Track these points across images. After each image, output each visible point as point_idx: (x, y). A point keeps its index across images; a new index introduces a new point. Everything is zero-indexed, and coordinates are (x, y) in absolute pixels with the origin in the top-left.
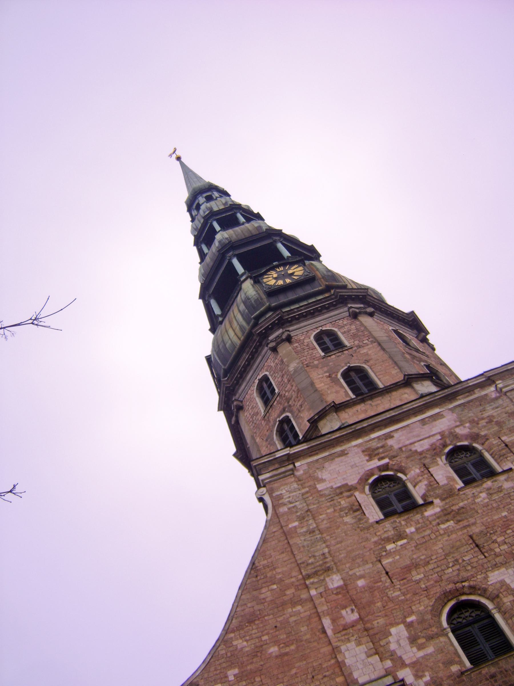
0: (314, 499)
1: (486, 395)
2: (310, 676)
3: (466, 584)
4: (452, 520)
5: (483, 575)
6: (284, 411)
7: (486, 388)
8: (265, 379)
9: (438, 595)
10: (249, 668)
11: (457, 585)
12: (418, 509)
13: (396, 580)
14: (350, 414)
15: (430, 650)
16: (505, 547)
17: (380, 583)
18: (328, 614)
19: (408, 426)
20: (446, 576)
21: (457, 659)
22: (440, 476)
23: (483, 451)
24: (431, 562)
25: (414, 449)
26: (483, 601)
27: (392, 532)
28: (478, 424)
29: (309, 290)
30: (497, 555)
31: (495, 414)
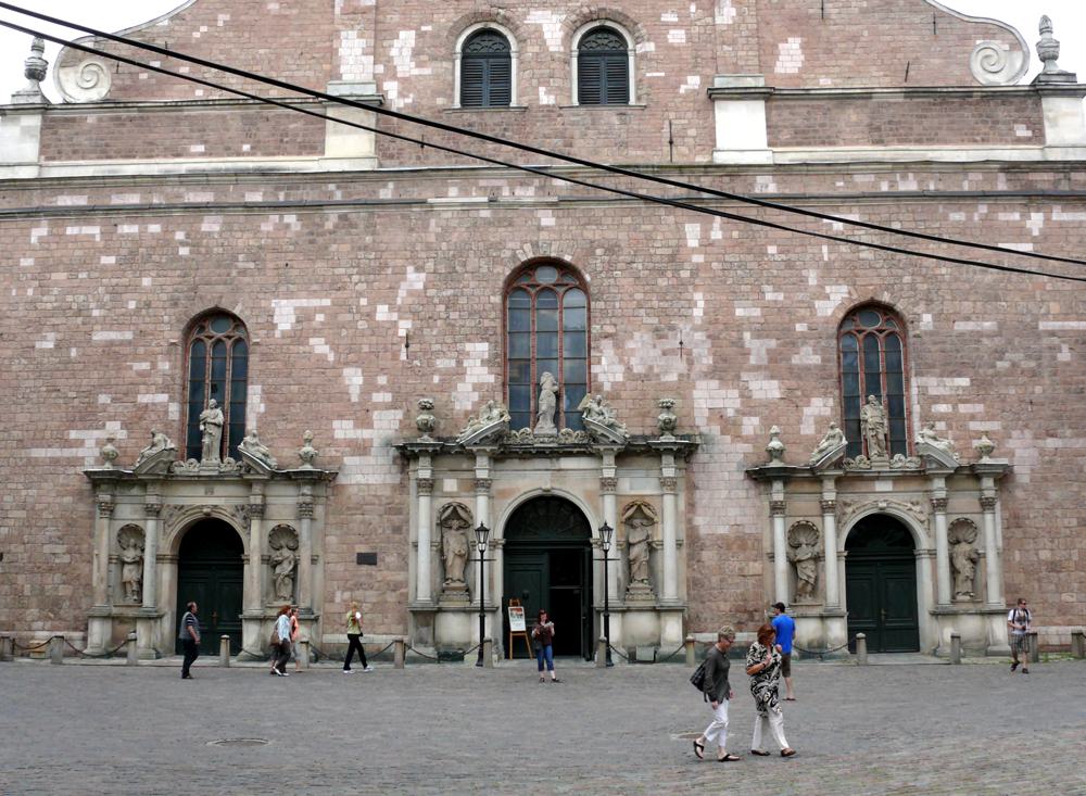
2: (299, 52)
5: (524, 10)
9: (467, 12)
15: (427, 71)
21: (449, 92)
26: (510, 38)
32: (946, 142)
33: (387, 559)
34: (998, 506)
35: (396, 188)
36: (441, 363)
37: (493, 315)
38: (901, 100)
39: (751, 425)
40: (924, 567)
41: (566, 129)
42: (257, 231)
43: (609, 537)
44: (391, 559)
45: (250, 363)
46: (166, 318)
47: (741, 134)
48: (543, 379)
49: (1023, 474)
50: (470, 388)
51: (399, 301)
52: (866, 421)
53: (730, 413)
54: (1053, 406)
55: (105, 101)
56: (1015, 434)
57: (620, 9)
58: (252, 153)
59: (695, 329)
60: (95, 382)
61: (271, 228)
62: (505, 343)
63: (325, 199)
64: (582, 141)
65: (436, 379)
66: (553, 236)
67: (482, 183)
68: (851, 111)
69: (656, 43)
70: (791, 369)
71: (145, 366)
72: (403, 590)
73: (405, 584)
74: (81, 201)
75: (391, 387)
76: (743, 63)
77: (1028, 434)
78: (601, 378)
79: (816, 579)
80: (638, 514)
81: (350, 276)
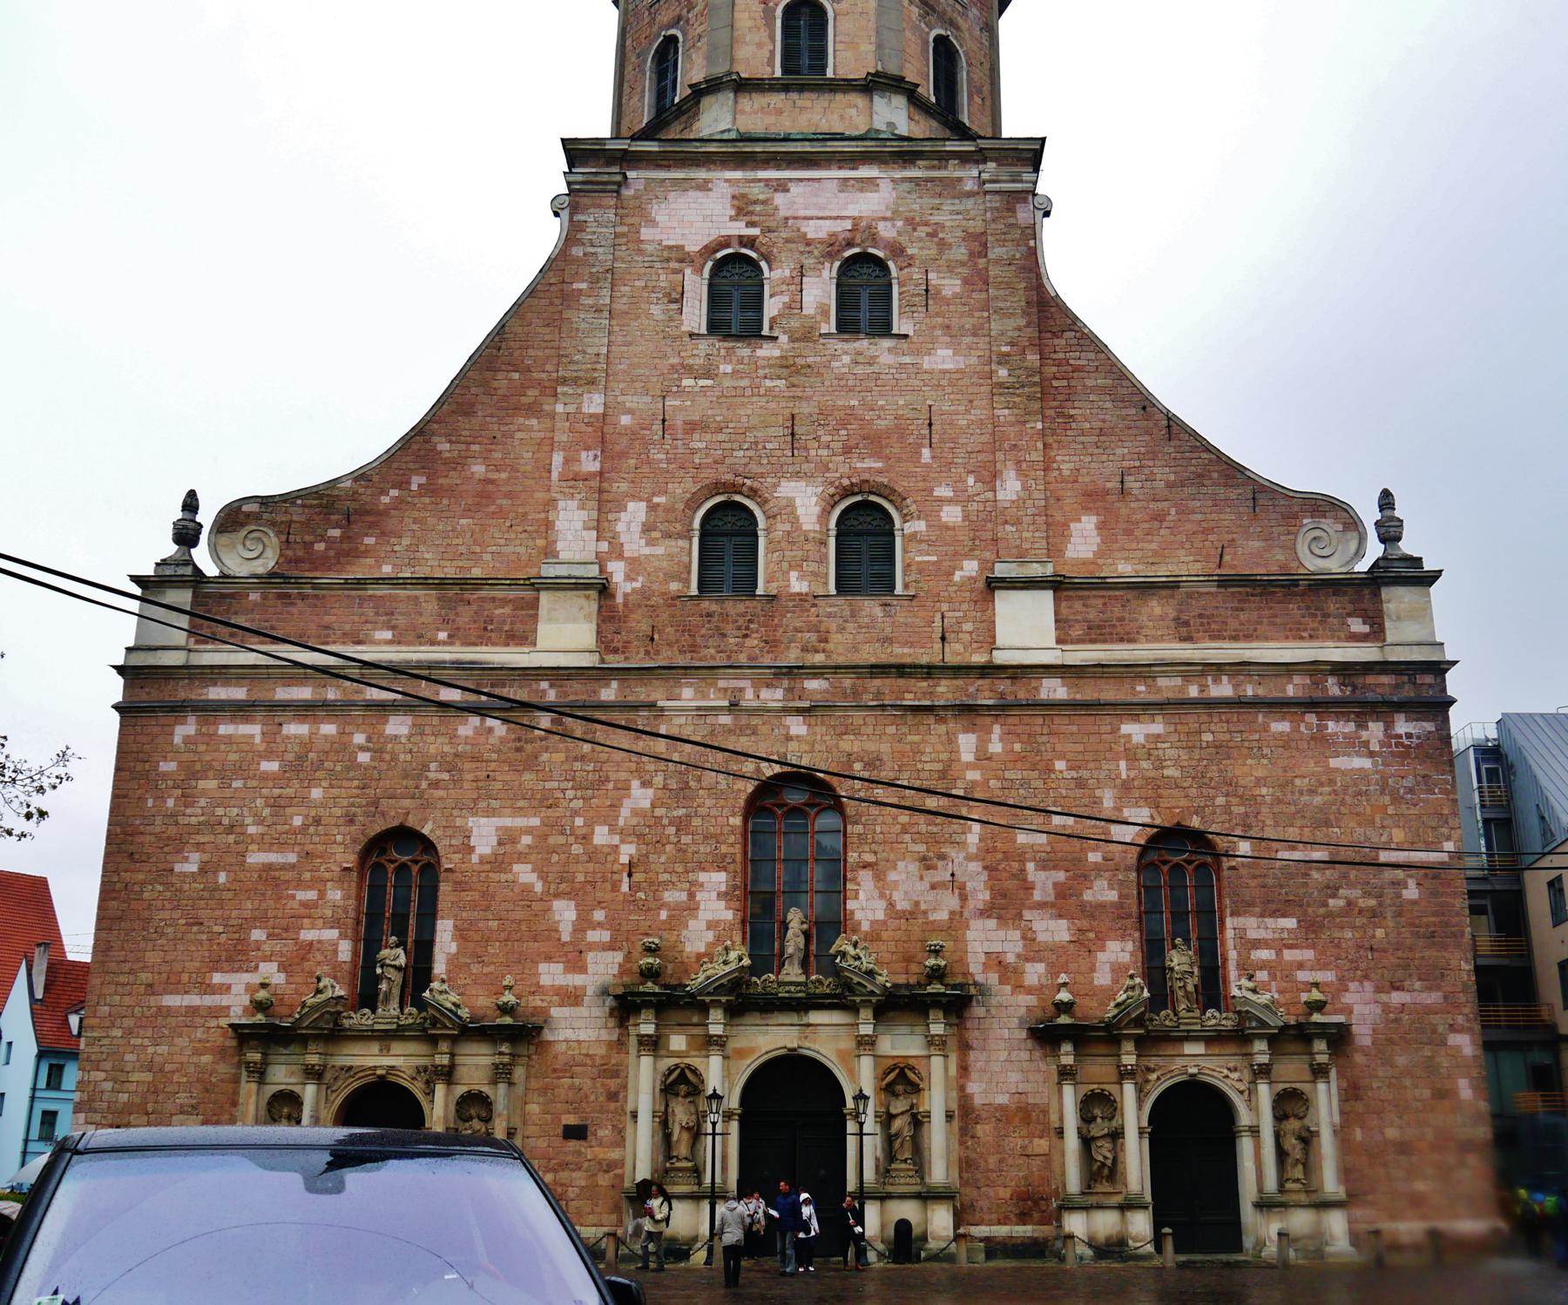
1: (960, 179)
10: (441, 481)
15: (660, 550)
16: (824, 452)
20: (731, 460)
22: (811, 298)
23: (894, 282)
25: (803, 229)
28: (915, 230)
31: (948, 224)
32: (1267, 639)
33: (600, 1133)
34: (1333, 1074)
35: (620, 689)
36: (670, 896)
37: (732, 839)
38: (1214, 590)
39: (1035, 973)
40: (1245, 1146)
42: (453, 736)
43: (865, 1106)
44: (605, 1133)
45: (440, 893)
46: (339, 838)
47: (1026, 628)
48: (790, 916)
49: (1363, 1034)
50: (703, 926)
51: (621, 822)
52: (1172, 969)
53: (1010, 958)
54: (1400, 953)
55: (272, 575)
56: (1353, 986)
57: (885, 481)
58: (451, 640)
59: (969, 858)
60: (247, 914)
61: (470, 733)
62: (746, 873)
63: (535, 700)
65: (664, 915)
66: (805, 747)
67: (722, 684)
68: (1154, 603)
70: (1083, 906)
71: (311, 895)
72: (618, 1171)
73: (620, 1163)
74: (239, 693)
75: (611, 924)
77: (1368, 986)
78: (858, 916)
79: (1115, 1160)
80: (901, 1080)
81: (563, 791)
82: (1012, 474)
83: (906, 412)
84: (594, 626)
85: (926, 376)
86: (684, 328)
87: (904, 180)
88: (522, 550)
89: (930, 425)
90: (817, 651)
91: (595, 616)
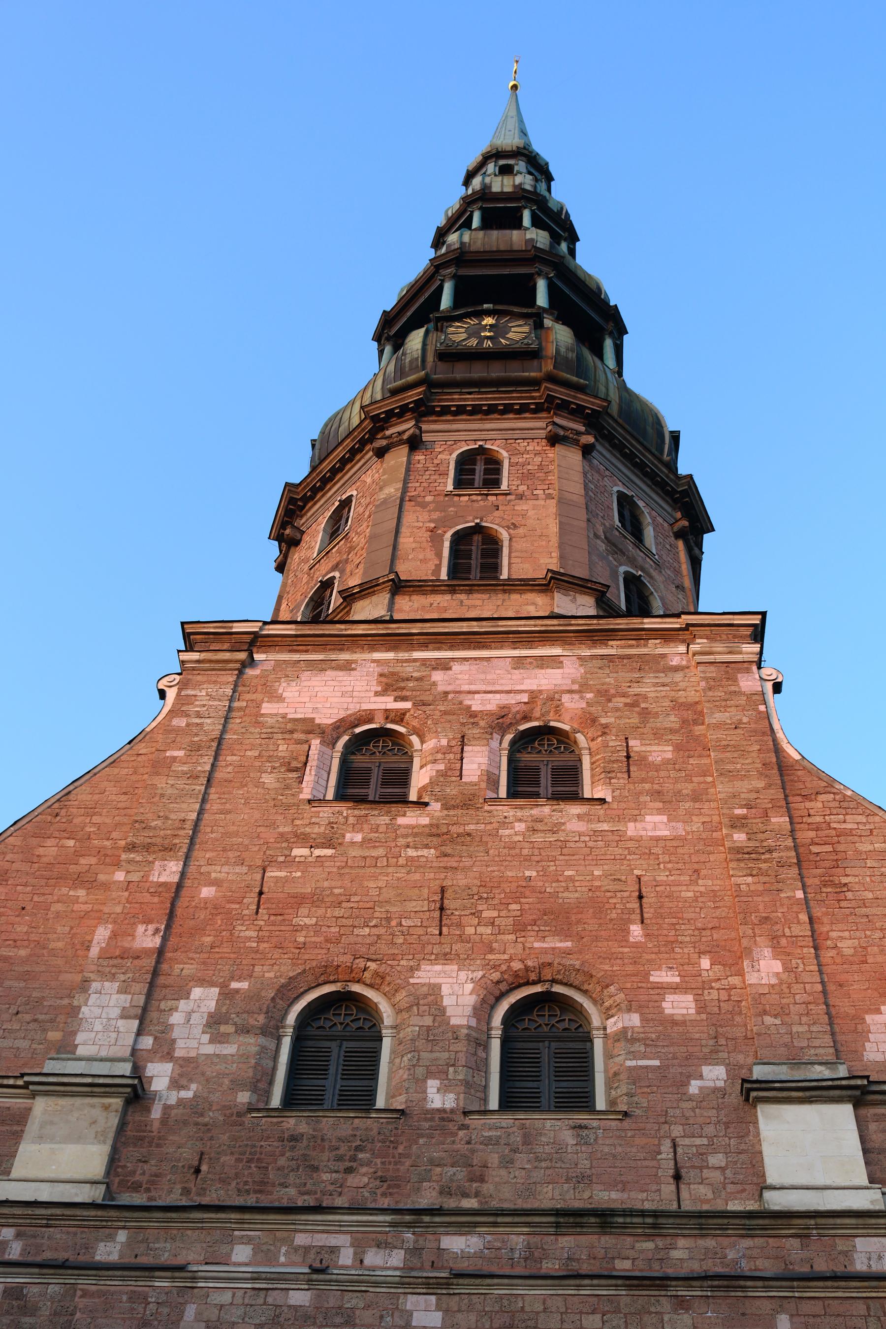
0: (242, 725)
1: (663, 656)
2: (13, 1010)
3: (372, 966)
4: (435, 848)
6: (335, 568)
7: (672, 645)
8: (346, 503)
9: (314, 964)
11: (357, 961)
12: (394, 808)
13: (265, 911)
14: (416, 605)
15: (229, 1049)
17: (238, 906)
18: (115, 922)
19: (488, 659)
20: (352, 939)
22: (475, 766)
23: (585, 752)
24: (344, 905)
25: (467, 702)
27: (322, 829)
28: (610, 701)
29: (516, 371)
30: (461, 938)
41: (473, 1151)
57: (577, 964)
64: (503, 1172)
67: (301, 1239)
69: (641, 1014)
76: (804, 1044)
82: (767, 952)
83: (606, 884)
84: (106, 1149)
85: (630, 844)
86: (302, 796)
87: (593, 657)
88: (23, 1044)
89: (640, 897)
90: (465, 1195)
91: (111, 1135)
